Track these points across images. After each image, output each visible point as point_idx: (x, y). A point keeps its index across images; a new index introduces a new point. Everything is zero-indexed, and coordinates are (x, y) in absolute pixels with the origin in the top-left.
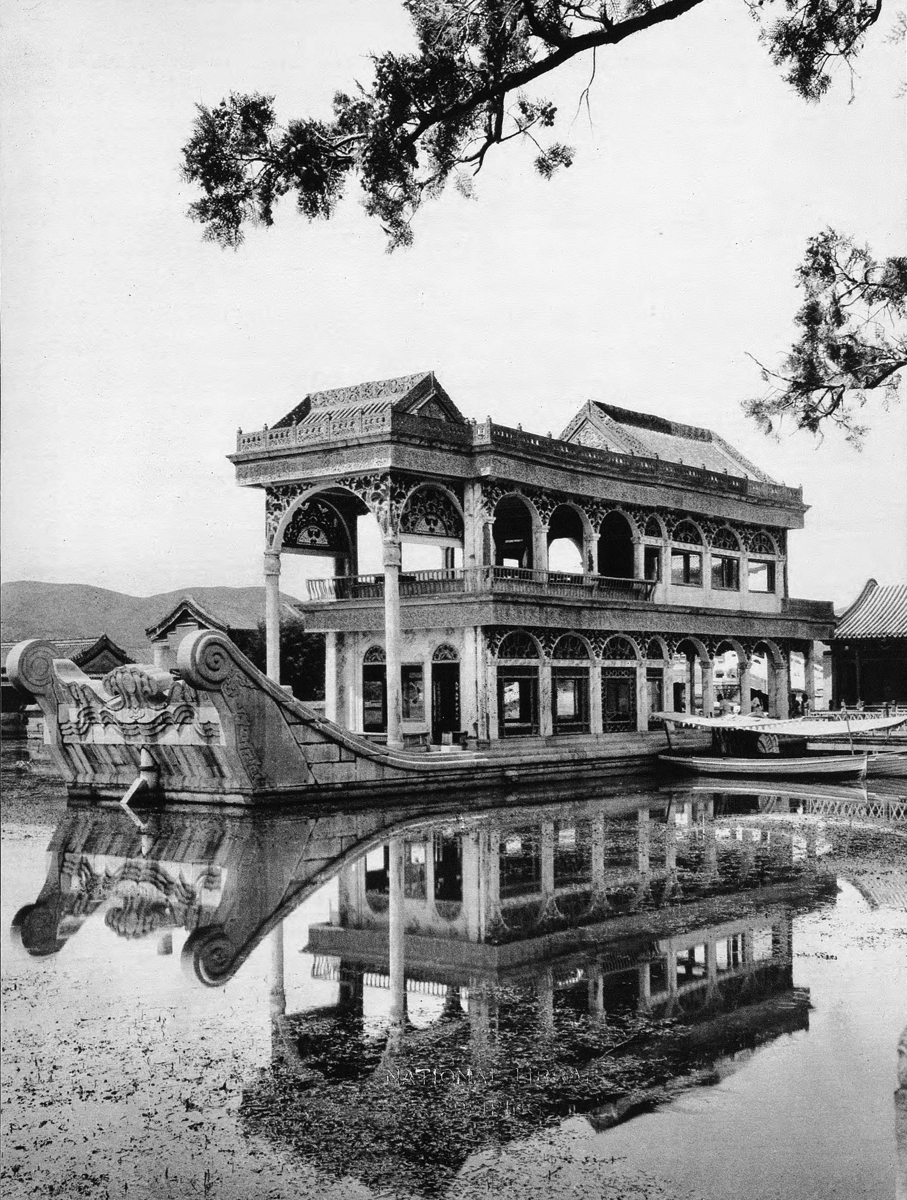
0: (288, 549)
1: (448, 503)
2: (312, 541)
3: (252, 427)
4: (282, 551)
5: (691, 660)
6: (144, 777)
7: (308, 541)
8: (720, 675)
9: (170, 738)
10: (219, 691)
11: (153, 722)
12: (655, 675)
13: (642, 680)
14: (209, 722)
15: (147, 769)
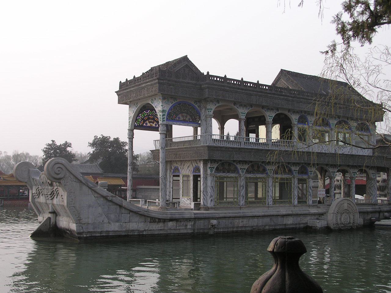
0: (137, 128)
1: (194, 108)
2: (150, 125)
3: (123, 81)
4: (135, 129)
5: (344, 175)
6: (50, 215)
7: (149, 125)
8: (378, 182)
9: (55, 201)
10: (60, 183)
11: (51, 194)
12: (301, 181)
13: (295, 183)
14: (62, 196)
15: (50, 213)
